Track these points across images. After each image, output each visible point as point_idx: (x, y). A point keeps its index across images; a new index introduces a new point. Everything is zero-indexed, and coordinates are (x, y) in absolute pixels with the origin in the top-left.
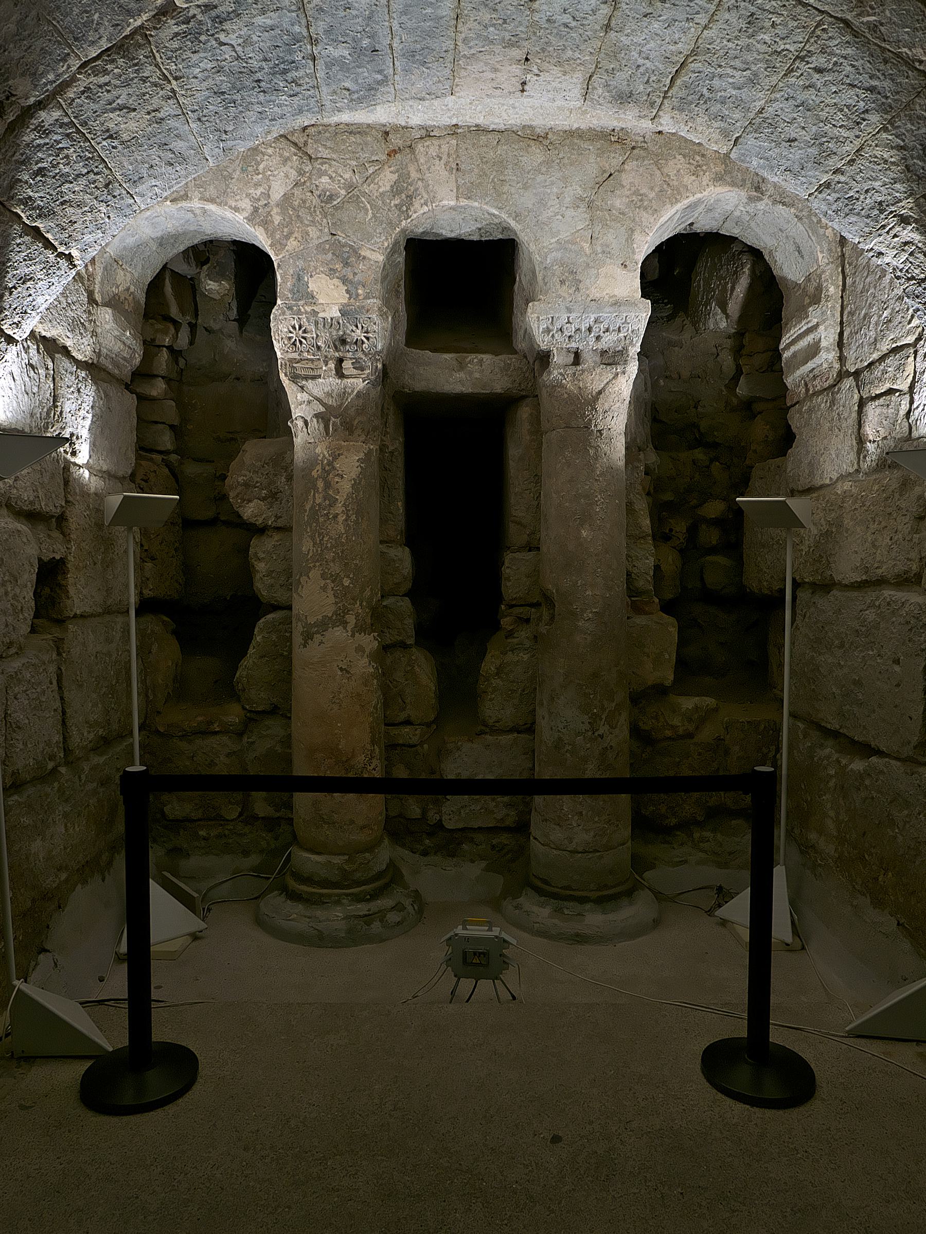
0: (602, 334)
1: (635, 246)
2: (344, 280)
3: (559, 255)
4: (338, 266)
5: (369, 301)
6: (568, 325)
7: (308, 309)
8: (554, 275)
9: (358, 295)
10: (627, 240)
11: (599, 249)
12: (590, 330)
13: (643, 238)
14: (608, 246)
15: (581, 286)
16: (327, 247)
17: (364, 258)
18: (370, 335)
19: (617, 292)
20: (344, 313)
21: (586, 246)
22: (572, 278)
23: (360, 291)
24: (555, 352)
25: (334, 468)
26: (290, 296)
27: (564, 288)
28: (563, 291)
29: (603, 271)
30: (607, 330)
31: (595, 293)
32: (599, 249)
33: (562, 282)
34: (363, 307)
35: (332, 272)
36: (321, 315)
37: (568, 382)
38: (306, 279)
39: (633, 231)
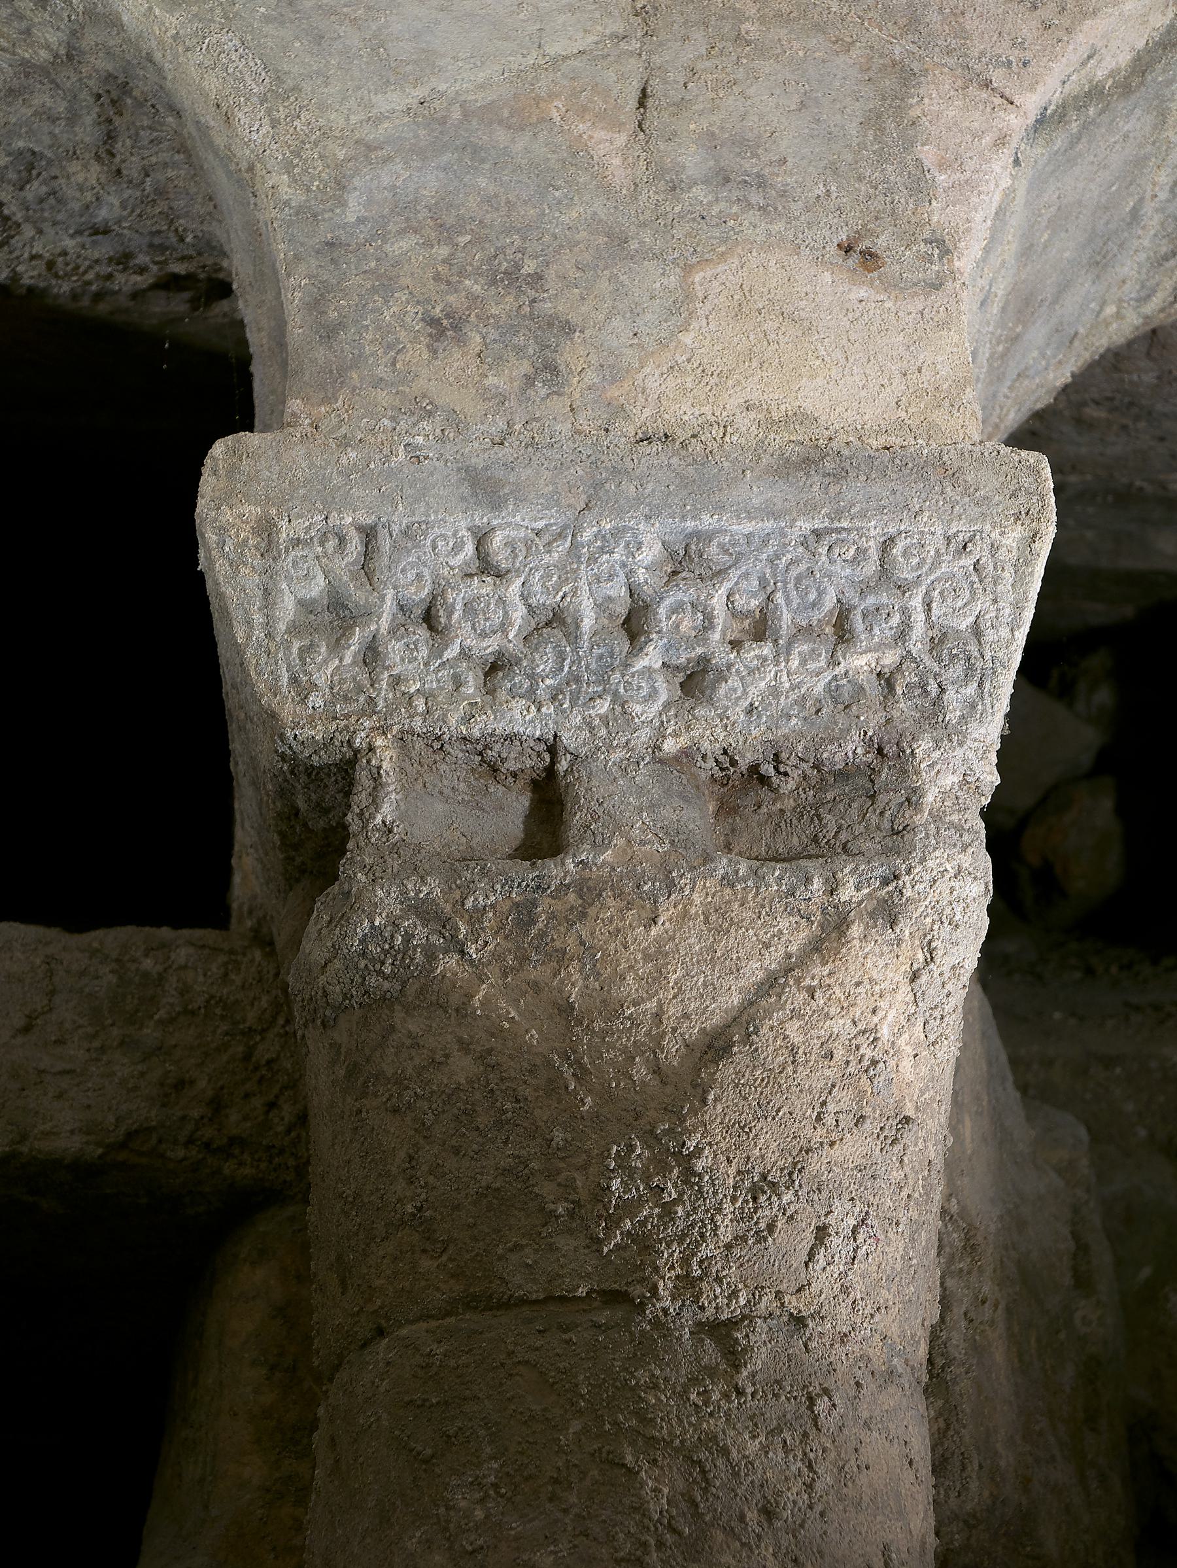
0: (722, 655)
1: (927, 154)
3: (428, 182)
6: (482, 587)
8: (386, 285)
10: (873, 120)
11: (691, 159)
12: (635, 624)
13: (976, 120)
14: (744, 145)
15: (571, 355)
19: (811, 396)
21: (610, 147)
22: (507, 295)
24: (387, 757)
27: (456, 360)
28: (450, 376)
29: (716, 281)
30: (761, 628)
31: (665, 394)
32: (691, 159)
33: (443, 329)
37: (478, 972)
39: (908, 76)
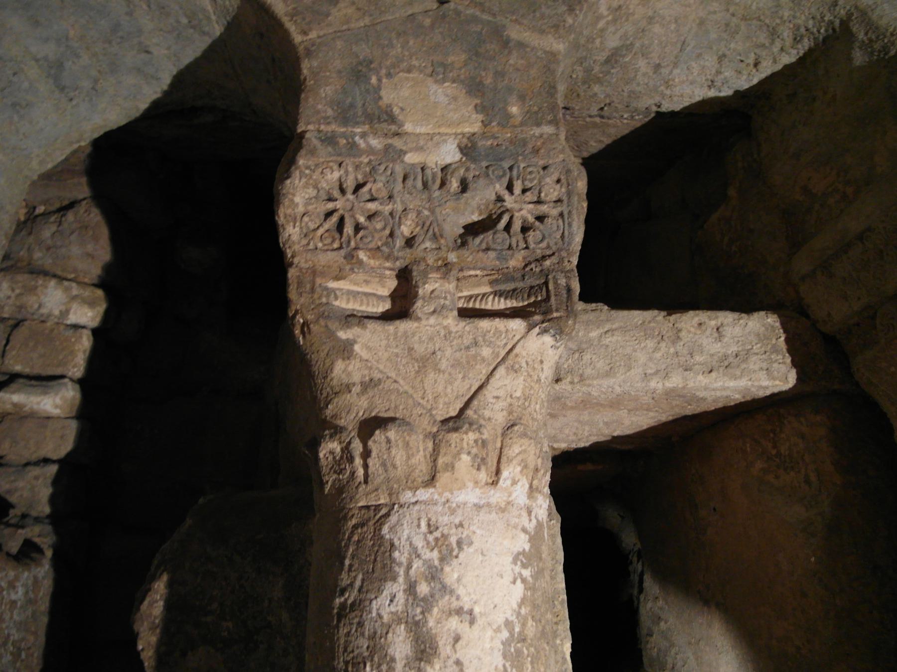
2: (474, 87)
4: (457, 58)
5: (537, 131)
7: (375, 143)
9: (509, 116)
16: (428, 22)
17: (521, 45)
18: (544, 208)
20: (468, 149)
23: (514, 110)
25: (445, 589)
26: (330, 112)
34: (524, 143)
35: (439, 71)
36: (411, 158)
38: (374, 80)
